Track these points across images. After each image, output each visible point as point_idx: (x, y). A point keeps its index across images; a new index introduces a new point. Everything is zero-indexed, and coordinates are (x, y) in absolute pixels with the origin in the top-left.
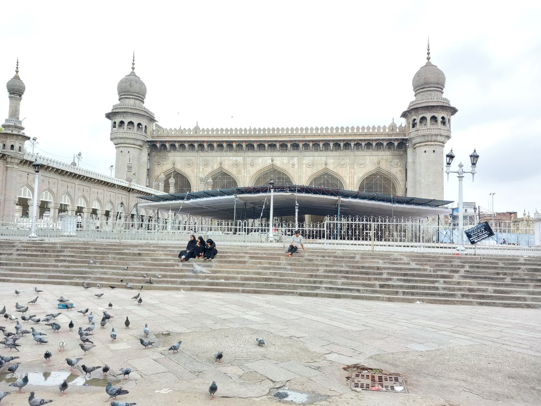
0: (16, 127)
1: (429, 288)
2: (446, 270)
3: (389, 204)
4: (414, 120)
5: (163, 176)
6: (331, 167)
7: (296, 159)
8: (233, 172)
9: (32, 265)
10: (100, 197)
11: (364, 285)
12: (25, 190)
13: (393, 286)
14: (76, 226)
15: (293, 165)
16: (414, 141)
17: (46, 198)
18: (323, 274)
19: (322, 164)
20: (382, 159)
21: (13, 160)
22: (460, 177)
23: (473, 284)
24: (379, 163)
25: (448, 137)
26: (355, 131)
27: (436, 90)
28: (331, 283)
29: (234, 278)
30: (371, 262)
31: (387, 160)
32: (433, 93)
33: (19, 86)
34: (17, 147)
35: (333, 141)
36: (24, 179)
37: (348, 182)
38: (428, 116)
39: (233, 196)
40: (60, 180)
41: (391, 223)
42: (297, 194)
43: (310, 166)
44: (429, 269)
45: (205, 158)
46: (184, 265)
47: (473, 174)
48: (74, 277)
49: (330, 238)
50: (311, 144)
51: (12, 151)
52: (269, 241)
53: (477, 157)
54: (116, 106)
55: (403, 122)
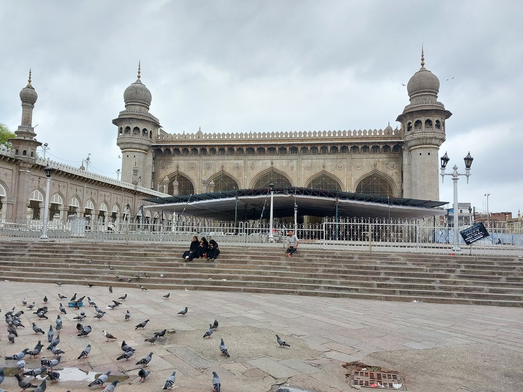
0: (28, 133)
1: (426, 287)
2: (442, 270)
3: (387, 206)
4: (410, 123)
5: (167, 179)
6: (329, 170)
7: (295, 161)
8: (234, 174)
9: (43, 265)
10: (108, 199)
11: (362, 284)
12: (37, 193)
13: (390, 286)
14: (84, 227)
15: (292, 168)
16: (409, 144)
17: (56, 201)
18: (322, 274)
19: (320, 167)
20: (379, 161)
21: (25, 165)
22: (455, 180)
23: (469, 283)
24: (375, 165)
25: (443, 140)
26: (352, 135)
27: (430, 95)
28: (330, 282)
29: (236, 278)
30: (368, 262)
31: (383, 163)
32: (427, 98)
33: (32, 95)
34: (29, 152)
35: (330, 144)
36: (36, 183)
37: (345, 184)
38: (423, 120)
39: (234, 198)
40: (69, 183)
41: (388, 224)
42: (296, 196)
43: (310, 168)
44: (425, 268)
45: (208, 162)
46: (187, 265)
47: (468, 176)
48: (83, 277)
49: (328, 239)
50: (309, 148)
51: (24, 156)
52: (269, 241)
53: (471, 159)
54: (122, 112)
55: (398, 125)
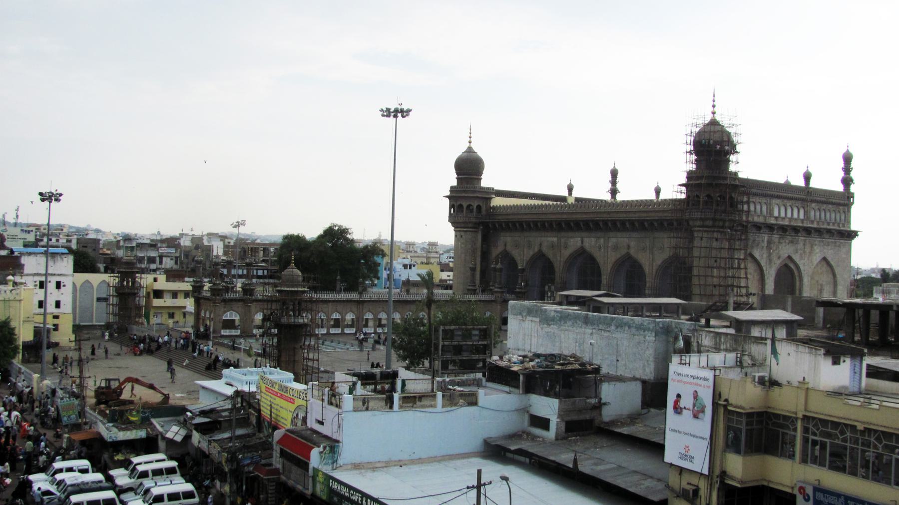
6: (632, 252)
7: (602, 241)
15: (600, 248)
43: (616, 248)
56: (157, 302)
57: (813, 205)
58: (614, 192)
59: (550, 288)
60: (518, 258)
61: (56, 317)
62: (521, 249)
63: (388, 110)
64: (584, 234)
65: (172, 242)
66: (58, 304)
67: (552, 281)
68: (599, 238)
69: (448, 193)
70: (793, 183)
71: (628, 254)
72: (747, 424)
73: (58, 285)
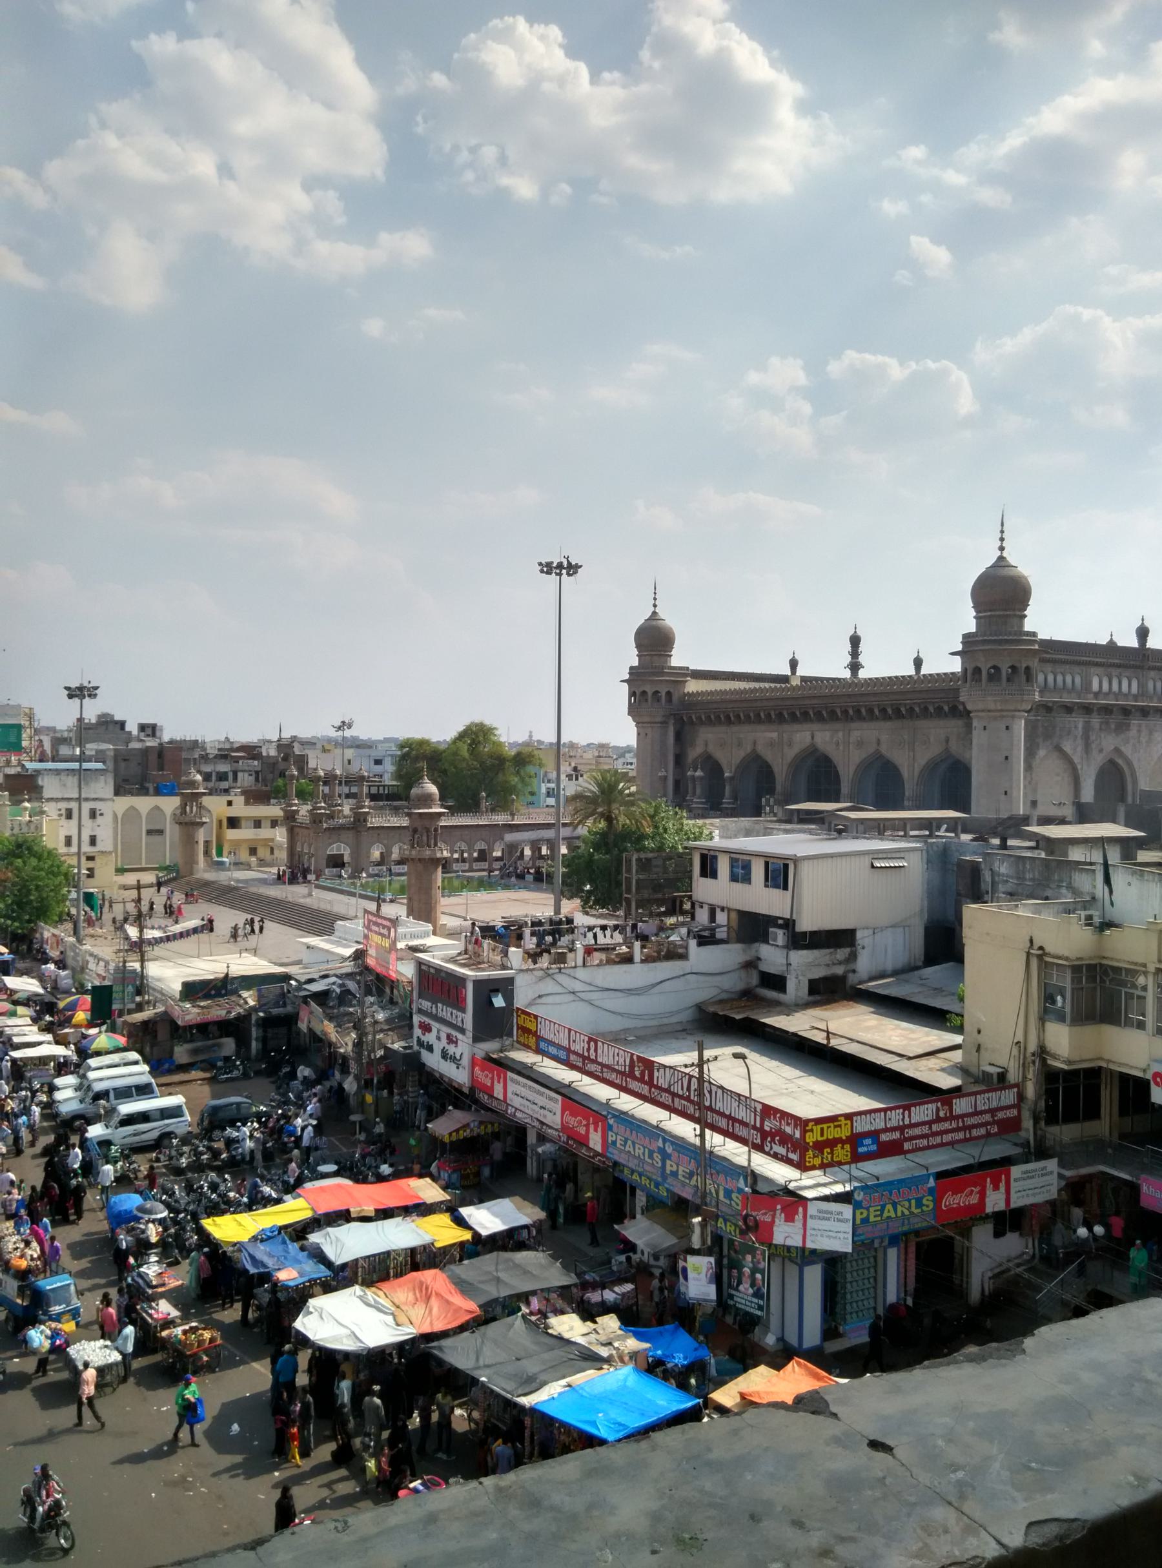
6: (884, 749)
7: (840, 734)
15: (838, 744)
43: (860, 744)
56: (231, 834)
57: (1152, 674)
58: (855, 667)
59: (768, 801)
60: (724, 762)
61: (90, 858)
62: (728, 747)
63: (549, 565)
64: (816, 726)
65: (251, 751)
66: (93, 841)
67: (771, 791)
68: (837, 731)
69: (627, 677)
70: (1119, 644)
71: (877, 752)
72: (1073, 981)
73: (93, 814)
